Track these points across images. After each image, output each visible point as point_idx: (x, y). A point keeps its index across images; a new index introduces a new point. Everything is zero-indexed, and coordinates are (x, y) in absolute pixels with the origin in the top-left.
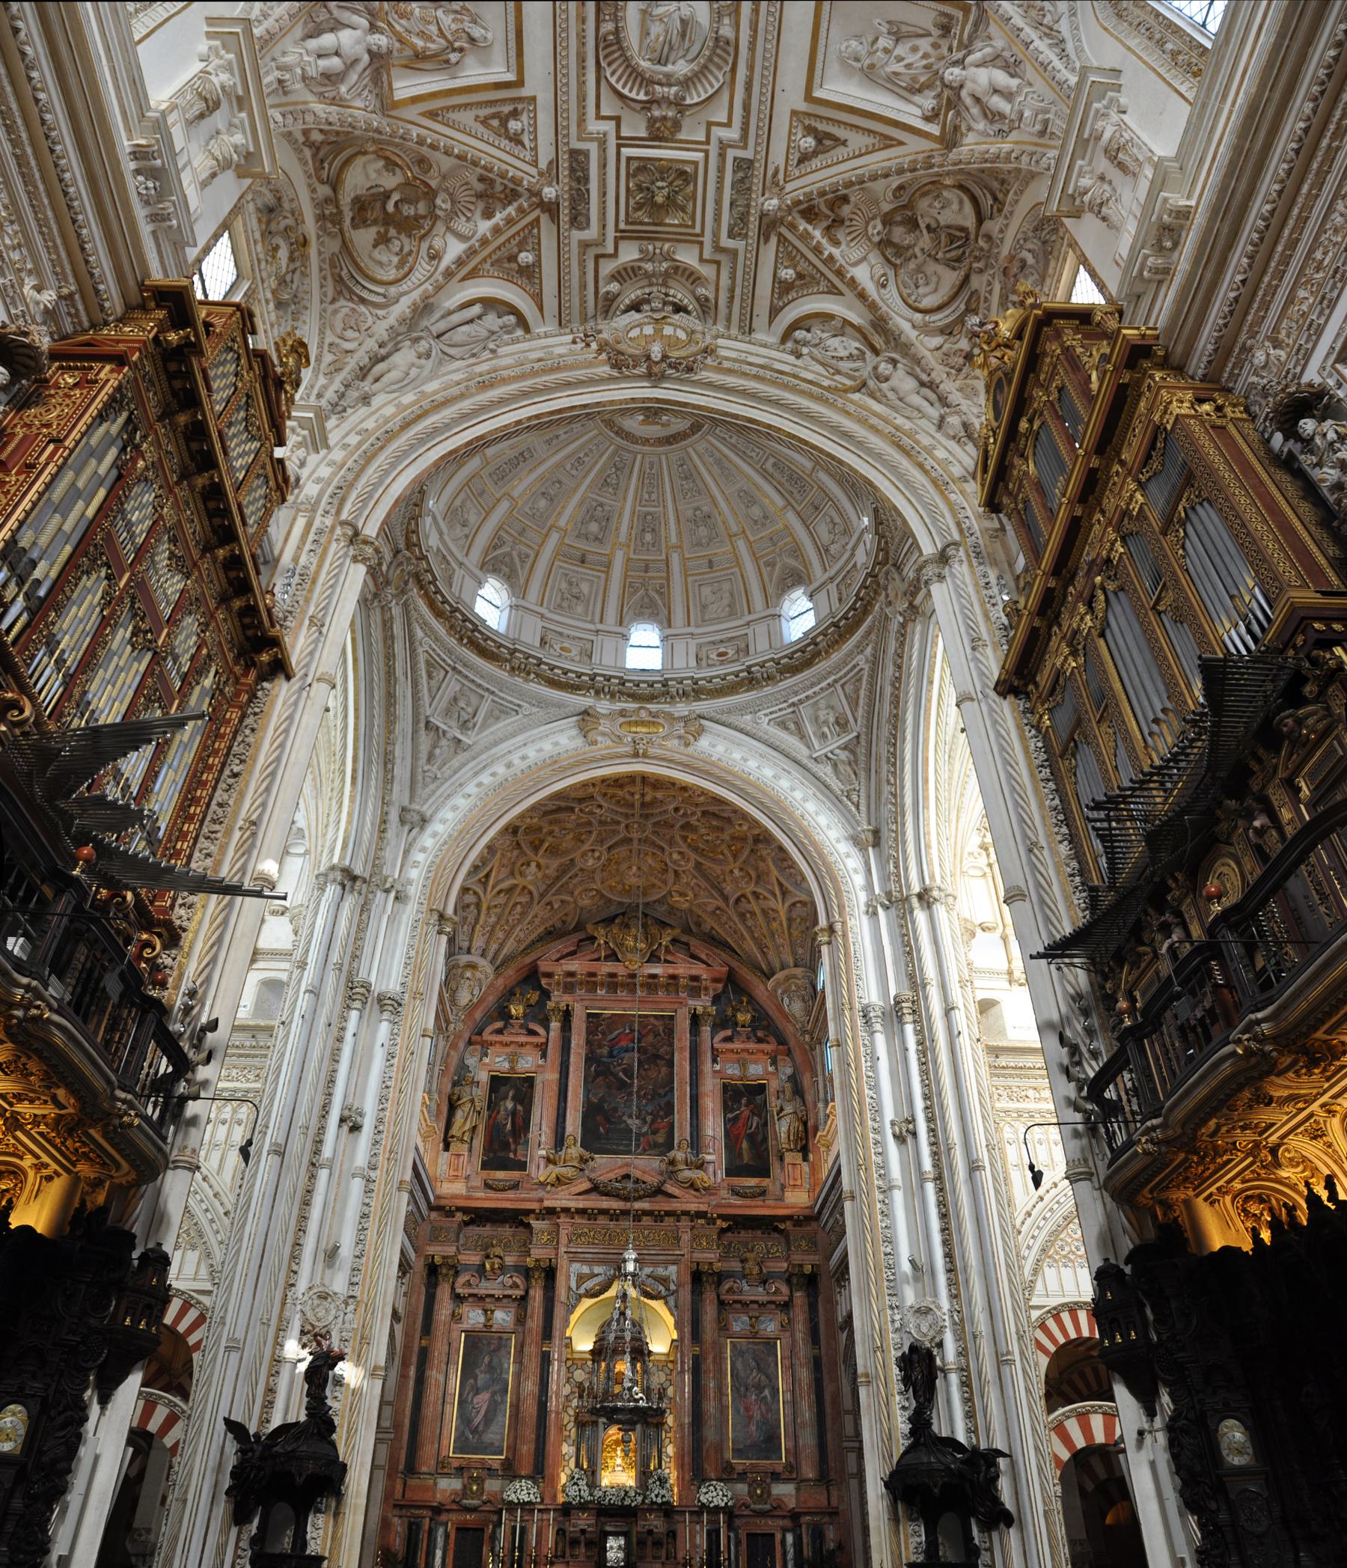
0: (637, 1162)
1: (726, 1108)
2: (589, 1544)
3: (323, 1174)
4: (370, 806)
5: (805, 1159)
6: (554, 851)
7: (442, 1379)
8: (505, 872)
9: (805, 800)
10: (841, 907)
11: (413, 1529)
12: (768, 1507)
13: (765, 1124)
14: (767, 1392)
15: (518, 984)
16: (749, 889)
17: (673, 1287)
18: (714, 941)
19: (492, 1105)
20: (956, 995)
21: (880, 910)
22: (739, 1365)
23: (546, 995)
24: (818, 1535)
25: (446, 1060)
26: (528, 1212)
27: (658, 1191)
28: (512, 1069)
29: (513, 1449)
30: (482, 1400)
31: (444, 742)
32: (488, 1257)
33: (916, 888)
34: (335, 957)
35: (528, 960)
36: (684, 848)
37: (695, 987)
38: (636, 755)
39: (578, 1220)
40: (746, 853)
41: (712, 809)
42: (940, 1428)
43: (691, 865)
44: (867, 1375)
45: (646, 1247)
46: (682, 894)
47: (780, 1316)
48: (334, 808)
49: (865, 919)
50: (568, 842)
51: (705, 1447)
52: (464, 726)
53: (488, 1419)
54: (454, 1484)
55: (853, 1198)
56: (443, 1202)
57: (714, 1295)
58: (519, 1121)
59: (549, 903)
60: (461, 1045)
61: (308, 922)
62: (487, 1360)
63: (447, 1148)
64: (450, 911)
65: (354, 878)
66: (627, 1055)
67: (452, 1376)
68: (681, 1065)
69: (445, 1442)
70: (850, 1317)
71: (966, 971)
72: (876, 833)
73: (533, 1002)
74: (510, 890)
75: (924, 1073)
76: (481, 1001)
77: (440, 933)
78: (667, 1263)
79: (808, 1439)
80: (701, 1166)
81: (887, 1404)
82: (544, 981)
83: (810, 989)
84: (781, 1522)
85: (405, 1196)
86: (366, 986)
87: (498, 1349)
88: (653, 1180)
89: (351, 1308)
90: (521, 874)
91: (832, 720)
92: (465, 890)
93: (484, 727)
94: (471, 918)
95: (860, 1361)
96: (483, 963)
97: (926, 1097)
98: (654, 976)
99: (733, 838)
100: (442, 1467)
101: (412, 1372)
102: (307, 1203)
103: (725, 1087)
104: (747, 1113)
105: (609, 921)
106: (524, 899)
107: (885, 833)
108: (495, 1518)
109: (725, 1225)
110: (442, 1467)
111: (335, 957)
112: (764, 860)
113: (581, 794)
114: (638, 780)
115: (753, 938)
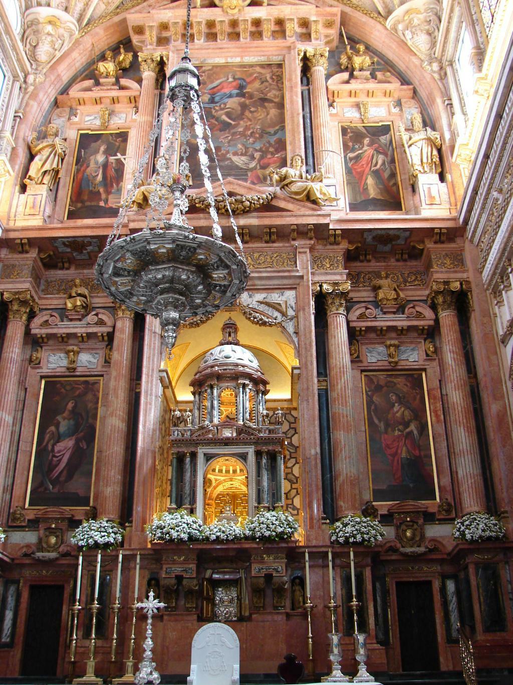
1: (346, 147)
5: (442, 178)
12: (422, 549)
13: (393, 161)
14: (413, 427)
15: (109, 49)
17: (291, 313)
27: (268, 207)
28: (103, 124)
30: (65, 447)
32: (70, 297)
35: (117, 19)
54: (30, 537)
56: (12, 235)
58: (112, 172)
62: (70, 406)
63: (24, 188)
68: (292, 102)
69: (17, 491)
73: (127, 64)
78: (281, 289)
82: (135, 39)
84: (437, 568)
87: (85, 393)
98: (257, 23)
103: (344, 131)
109: (352, 248)
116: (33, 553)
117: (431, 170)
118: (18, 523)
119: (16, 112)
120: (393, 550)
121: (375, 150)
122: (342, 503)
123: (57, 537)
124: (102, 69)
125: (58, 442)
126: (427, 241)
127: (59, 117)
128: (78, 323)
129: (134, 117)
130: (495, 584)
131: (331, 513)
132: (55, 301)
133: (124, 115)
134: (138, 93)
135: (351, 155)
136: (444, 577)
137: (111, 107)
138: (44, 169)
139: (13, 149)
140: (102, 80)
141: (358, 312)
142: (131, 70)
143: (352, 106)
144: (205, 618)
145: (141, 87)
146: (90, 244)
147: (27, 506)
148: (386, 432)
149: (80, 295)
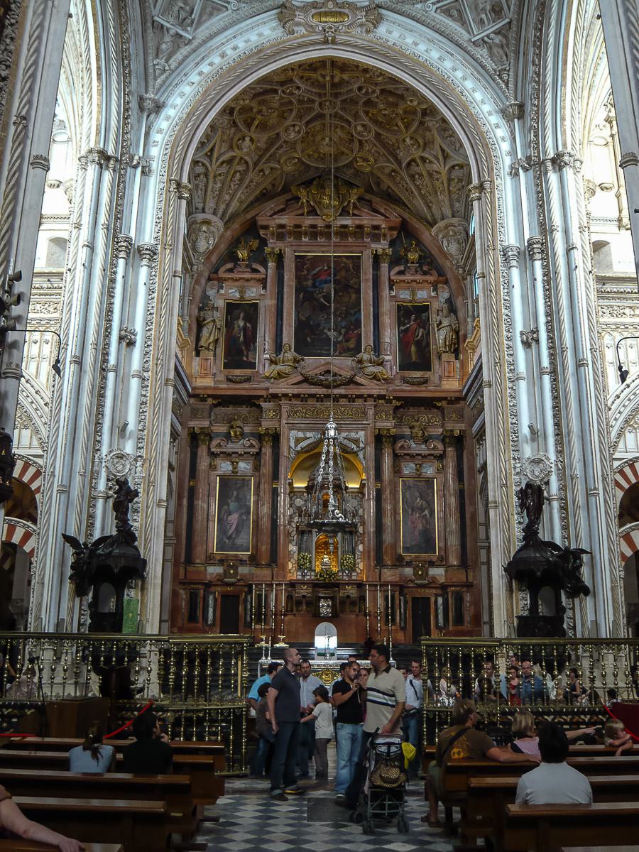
0: (336, 361)
1: (400, 323)
2: (308, 604)
3: (111, 376)
4: (114, 98)
5: (457, 358)
6: (263, 127)
7: (205, 506)
8: (225, 147)
9: (464, 79)
10: (490, 170)
11: (193, 598)
12: (426, 582)
14: (426, 512)
16: (417, 154)
17: (362, 445)
18: (391, 198)
19: (229, 325)
20: (576, 238)
21: (521, 171)
22: (408, 495)
23: (264, 242)
24: (459, 599)
25: (192, 292)
26: (258, 397)
27: (351, 381)
28: (242, 297)
29: (256, 548)
30: (234, 519)
31: (167, 38)
32: (232, 427)
33: (551, 154)
34: (102, 219)
35: (249, 216)
36: (367, 121)
37: (376, 234)
38: (326, 42)
39: (294, 402)
40: (416, 125)
41: (389, 87)
42: (544, 535)
43: (373, 134)
44: (495, 502)
45: (343, 419)
46: (366, 160)
47: (436, 464)
48: (86, 100)
49: (508, 178)
50: (273, 119)
51: (385, 546)
52: (182, 23)
53: (238, 531)
54: (219, 570)
55: (490, 386)
56: (198, 392)
57: (391, 450)
59: (262, 171)
60: (203, 281)
61: (79, 193)
62: (235, 493)
64: (185, 180)
65: (108, 158)
66: (326, 286)
67: (212, 504)
68: (366, 292)
69: (210, 545)
70: (485, 464)
71: (585, 219)
72: (521, 107)
74: (230, 161)
75: (548, 297)
76: (215, 247)
77: (180, 198)
78: (357, 430)
79: (454, 541)
80: (381, 364)
81: (508, 521)
82: (261, 232)
83: (463, 234)
84: (435, 591)
85: (171, 389)
86: (128, 240)
87: (243, 486)
88: (347, 374)
89: (139, 464)
90: (239, 148)
91: (488, 7)
92: (195, 163)
93: (200, 23)
94: (202, 186)
95: (491, 494)
96: (214, 219)
97: (548, 314)
98: (345, 227)
99: (405, 112)
100: (210, 559)
101: (185, 502)
102: (102, 396)
104: (415, 326)
105: (308, 184)
106: (241, 168)
107: (528, 107)
108: (246, 589)
109: (398, 404)
110: (210, 559)
111: (102, 219)
112: (429, 129)
113: (282, 78)
114: (329, 65)
115: (423, 196)
117: (450, 350)
118: (212, 562)
120: (412, 581)
121: (418, 324)
122: (385, 557)
123: (234, 570)
126: (444, 402)
129: (262, 292)
130: (461, 604)
131: (380, 562)
132: (221, 428)
133: (255, 290)
134: (264, 276)
135: (402, 328)
136: (437, 596)
137: (246, 284)
141: (399, 445)
142: (259, 256)
143: (405, 289)
144: (317, 618)
145: (267, 271)
148: (412, 514)
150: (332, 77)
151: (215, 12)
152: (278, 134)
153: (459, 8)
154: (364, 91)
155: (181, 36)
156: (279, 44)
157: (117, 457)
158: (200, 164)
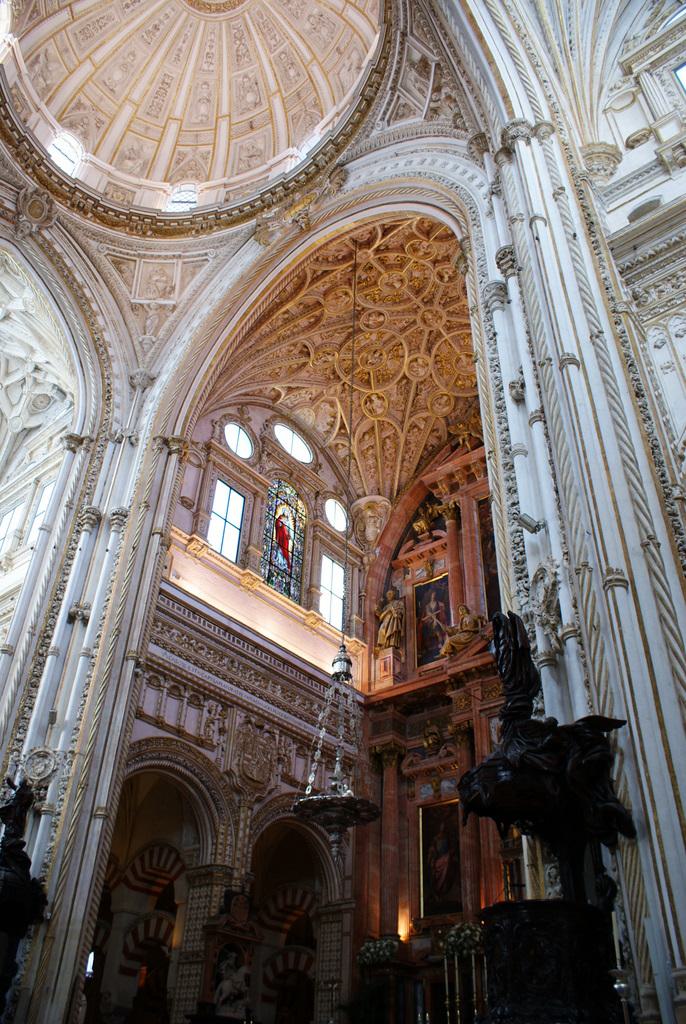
6: (384, 379)
28: (428, 575)
30: (444, 859)
35: (416, 482)
50: (390, 365)
56: (374, 699)
59: (414, 426)
62: (442, 826)
65: (80, 441)
82: (435, 492)
93: (183, 288)
96: (378, 498)
116: (427, 957)
119: (360, 592)
124: (417, 529)
125: (436, 859)
127: (397, 579)
128: (433, 758)
138: (388, 635)
139: (364, 624)
140: (420, 537)
142: (436, 522)
146: (428, 691)
147: (422, 916)
149: (432, 734)
150: (402, 281)
151: (197, 270)
152: (405, 377)
153: (404, 102)
154: (446, 279)
155: (165, 305)
156: (262, 258)
157: (39, 756)
158: (340, 446)
